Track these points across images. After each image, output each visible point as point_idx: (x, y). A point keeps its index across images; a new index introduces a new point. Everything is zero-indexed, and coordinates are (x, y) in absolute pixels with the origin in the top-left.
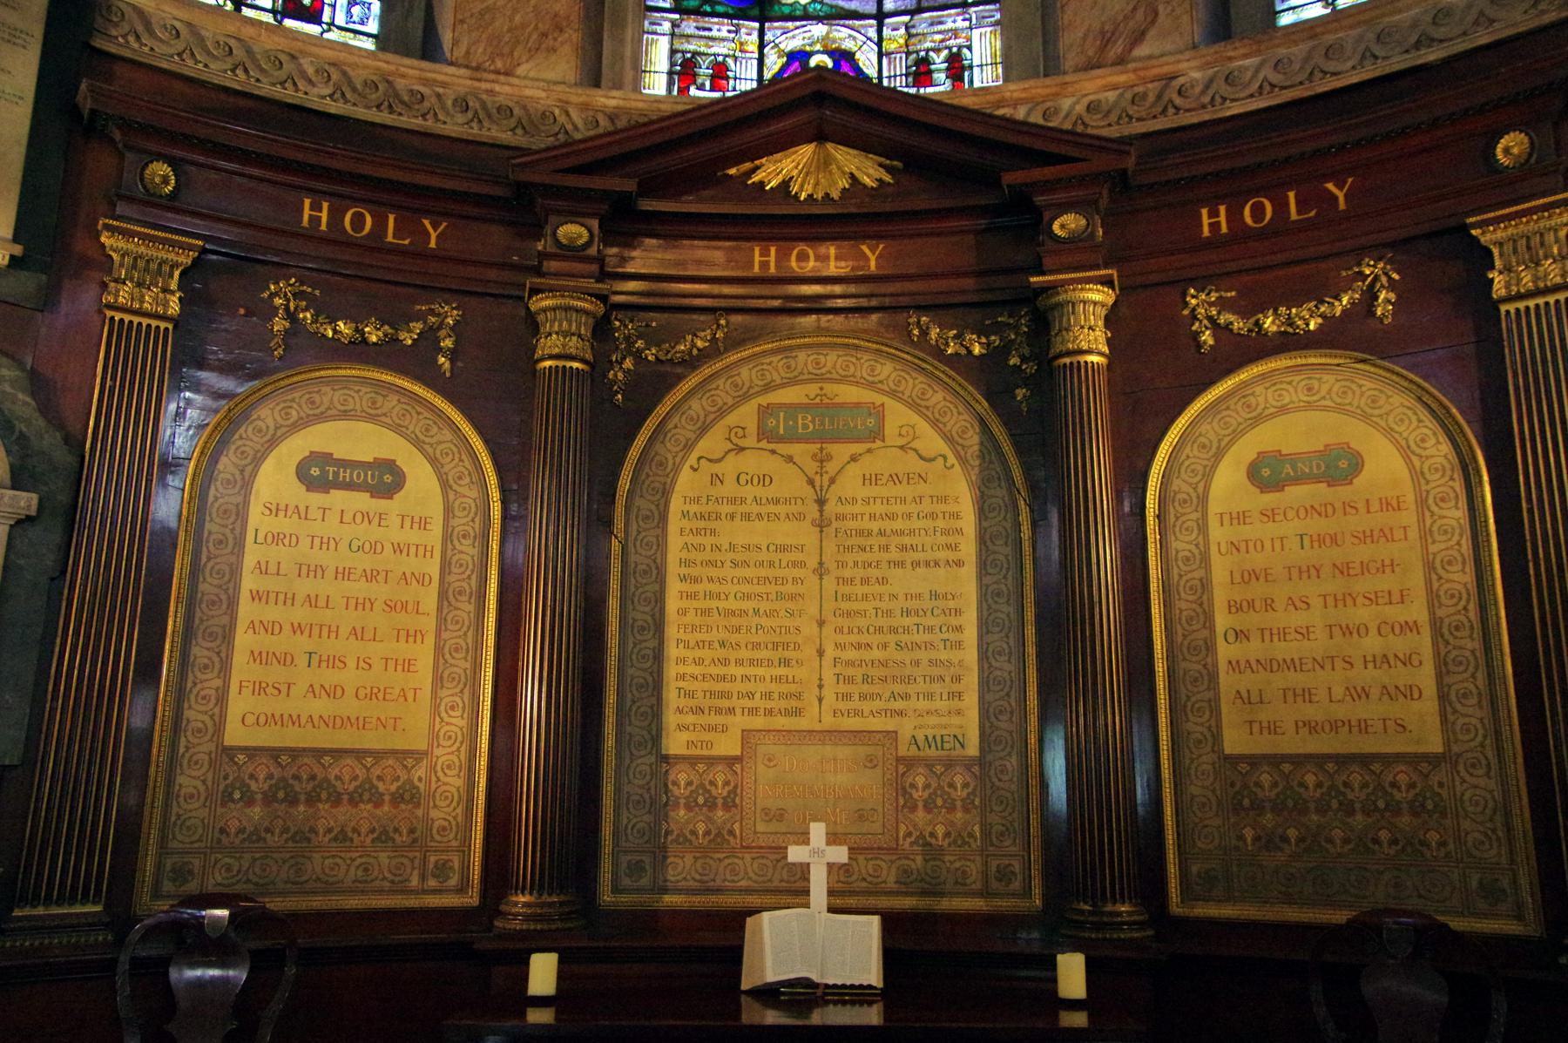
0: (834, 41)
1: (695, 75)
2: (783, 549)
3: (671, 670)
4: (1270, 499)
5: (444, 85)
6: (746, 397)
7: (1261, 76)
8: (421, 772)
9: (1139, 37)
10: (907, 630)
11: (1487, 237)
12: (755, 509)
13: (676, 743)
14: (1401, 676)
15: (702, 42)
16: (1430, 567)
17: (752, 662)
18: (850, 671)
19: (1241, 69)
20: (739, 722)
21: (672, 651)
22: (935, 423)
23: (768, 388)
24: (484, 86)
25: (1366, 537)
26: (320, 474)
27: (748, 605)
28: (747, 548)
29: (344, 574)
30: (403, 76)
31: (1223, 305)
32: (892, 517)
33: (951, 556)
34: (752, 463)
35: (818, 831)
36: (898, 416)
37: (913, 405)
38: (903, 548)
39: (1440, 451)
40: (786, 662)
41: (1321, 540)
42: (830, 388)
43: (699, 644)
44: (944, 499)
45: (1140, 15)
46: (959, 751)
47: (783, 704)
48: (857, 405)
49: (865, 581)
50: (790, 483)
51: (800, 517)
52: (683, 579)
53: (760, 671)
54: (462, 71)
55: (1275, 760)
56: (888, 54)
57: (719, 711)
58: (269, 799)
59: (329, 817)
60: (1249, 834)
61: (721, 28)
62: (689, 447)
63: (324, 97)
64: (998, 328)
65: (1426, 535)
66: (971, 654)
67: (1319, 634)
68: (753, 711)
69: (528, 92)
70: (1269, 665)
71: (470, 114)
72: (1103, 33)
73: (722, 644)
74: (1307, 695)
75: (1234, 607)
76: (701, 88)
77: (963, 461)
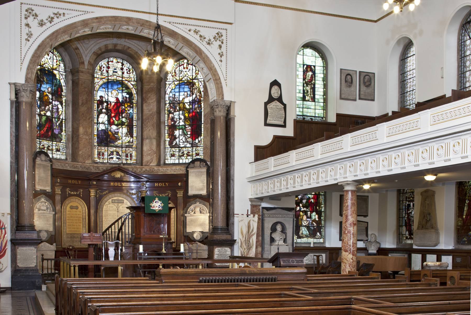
26: (72, 208)
50: (115, 207)
61: (103, 148)
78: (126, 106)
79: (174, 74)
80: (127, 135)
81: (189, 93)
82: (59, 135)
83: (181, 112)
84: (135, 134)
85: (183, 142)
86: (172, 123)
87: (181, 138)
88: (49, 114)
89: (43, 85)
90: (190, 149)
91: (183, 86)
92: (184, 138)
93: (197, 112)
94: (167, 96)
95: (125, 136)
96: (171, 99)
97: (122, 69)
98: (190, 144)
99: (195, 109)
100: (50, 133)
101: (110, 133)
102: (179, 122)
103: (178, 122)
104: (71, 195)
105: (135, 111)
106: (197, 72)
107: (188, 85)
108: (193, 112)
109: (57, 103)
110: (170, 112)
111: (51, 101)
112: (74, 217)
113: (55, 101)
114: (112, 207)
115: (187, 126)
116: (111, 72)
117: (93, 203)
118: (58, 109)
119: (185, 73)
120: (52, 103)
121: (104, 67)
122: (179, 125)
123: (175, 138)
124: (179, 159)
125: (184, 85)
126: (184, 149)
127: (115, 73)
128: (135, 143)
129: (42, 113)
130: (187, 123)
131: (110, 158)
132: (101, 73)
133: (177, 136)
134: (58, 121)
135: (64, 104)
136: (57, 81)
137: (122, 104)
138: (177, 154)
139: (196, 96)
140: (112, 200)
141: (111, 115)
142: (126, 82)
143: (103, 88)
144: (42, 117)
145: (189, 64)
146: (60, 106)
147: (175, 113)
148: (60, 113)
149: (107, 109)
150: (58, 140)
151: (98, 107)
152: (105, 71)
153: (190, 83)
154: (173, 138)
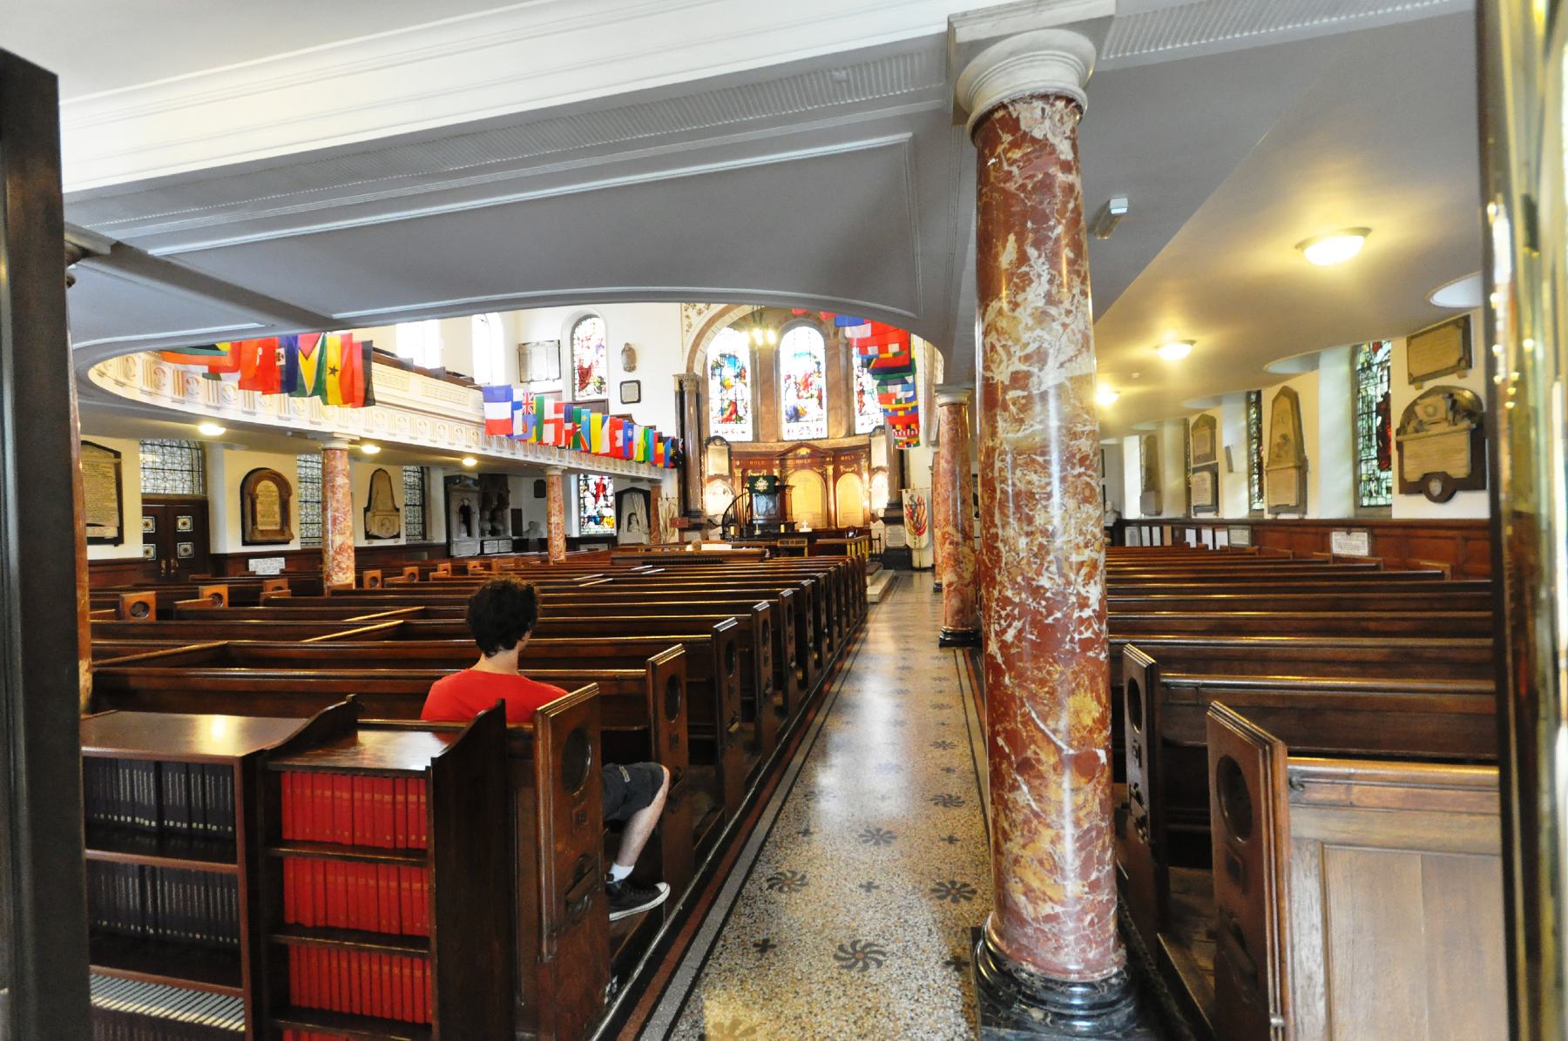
154: (862, 404)
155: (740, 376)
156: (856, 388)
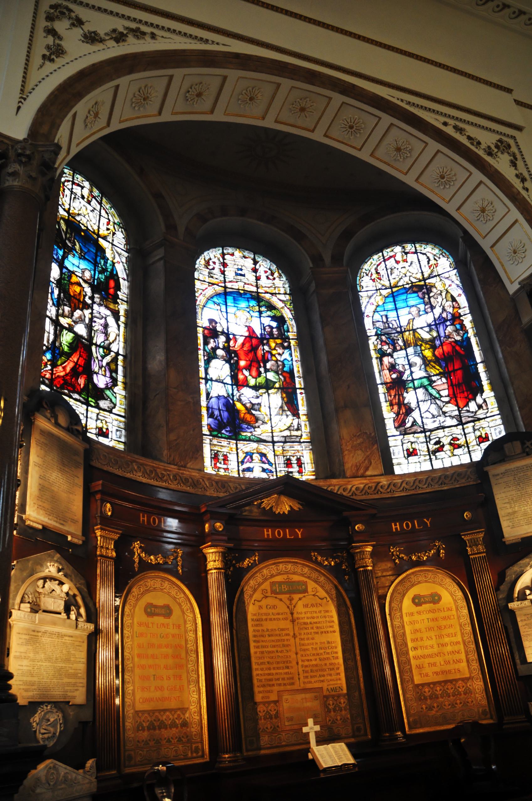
0: (260, 450)
1: (218, 459)
2: (282, 630)
3: (255, 673)
4: (419, 608)
5: (170, 471)
6: (266, 580)
7: (403, 486)
8: (187, 715)
9: (367, 469)
10: (321, 654)
11: (466, 538)
12: (273, 617)
13: (258, 698)
14: (457, 656)
15: (220, 447)
16: (461, 626)
17: (278, 668)
18: (307, 669)
19: (397, 483)
20: (276, 688)
21: (254, 666)
22: (322, 587)
23: (272, 576)
24: (181, 471)
25: (444, 618)
26: (151, 611)
27: (275, 649)
28: (272, 630)
29: (160, 646)
30: (159, 468)
31: (401, 552)
32: (313, 618)
33: (332, 629)
34: (270, 601)
35: (310, 721)
36: (311, 585)
37: (316, 582)
38: (317, 628)
39: (460, 594)
40: (287, 667)
41: (433, 620)
42: (291, 576)
43: (262, 663)
44: (327, 611)
45: (366, 462)
46: (341, 692)
47: (288, 681)
48: (299, 582)
49: (308, 639)
50: (282, 608)
51: (286, 619)
52: (255, 641)
53: (281, 671)
54: (175, 467)
55: (428, 684)
56: (277, 456)
57: (270, 685)
58: (149, 729)
59: (166, 733)
60: (424, 706)
61: (224, 443)
62: (251, 596)
63: (139, 476)
64: (338, 557)
65: (459, 618)
66: (341, 661)
67: (435, 646)
68: (280, 685)
69: (193, 474)
70: (424, 657)
71: (177, 481)
72: (356, 466)
73: (268, 663)
74: (434, 664)
75: (413, 640)
76: (220, 463)
77: (332, 599)
78: (273, 345)
79: (375, 276)
80: (283, 411)
81: (422, 307)
82: (108, 392)
83: (411, 350)
84: (303, 409)
85: (433, 416)
86: (394, 376)
87: (424, 406)
88: (81, 329)
89: (70, 257)
90: (458, 431)
91: (404, 297)
92: (433, 406)
93: (456, 341)
94: (368, 323)
95: (278, 414)
96: (380, 325)
97: (255, 270)
98: (452, 417)
99: (448, 337)
100: (82, 381)
101: (239, 406)
102: (412, 373)
103: (408, 372)
104: (145, 567)
105: (296, 355)
106: (432, 262)
107: (414, 292)
108: (442, 344)
109: (104, 311)
110: (382, 354)
111: (89, 302)
112: (160, 646)
113: (100, 305)
114: (274, 607)
115: (434, 378)
116: (230, 273)
117: (215, 591)
118: (106, 326)
119: (404, 271)
120: (90, 307)
121: (214, 263)
122: (413, 380)
123: (409, 411)
124: (431, 459)
125: (406, 292)
126: (440, 433)
127: (239, 277)
128: (305, 431)
129: (64, 321)
130: (433, 372)
131: (244, 470)
132: (209, 273)
133: (413, 405)
134: (106, 355)
135: (122, 319)
136: (106, 263)
137: (262, 340)
138: (422, 448)
139: (444, 310)
140: (272, 584)
141: (237, 362)
142: (268, 296)
143: (215, 303)
144: (61, 331)
145: (406, 253)
146: (111, 321)
147: (395, 355)
148: (111, 339)
149: (227, 349)
150: (103, 404)
151: (206, 343)
152: (217, 271)
153: (420, 288)
154: (404, 410)
155: (105, 289)
156: (381, 376)
